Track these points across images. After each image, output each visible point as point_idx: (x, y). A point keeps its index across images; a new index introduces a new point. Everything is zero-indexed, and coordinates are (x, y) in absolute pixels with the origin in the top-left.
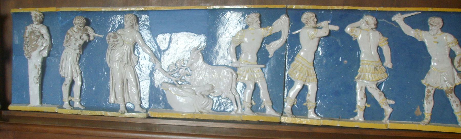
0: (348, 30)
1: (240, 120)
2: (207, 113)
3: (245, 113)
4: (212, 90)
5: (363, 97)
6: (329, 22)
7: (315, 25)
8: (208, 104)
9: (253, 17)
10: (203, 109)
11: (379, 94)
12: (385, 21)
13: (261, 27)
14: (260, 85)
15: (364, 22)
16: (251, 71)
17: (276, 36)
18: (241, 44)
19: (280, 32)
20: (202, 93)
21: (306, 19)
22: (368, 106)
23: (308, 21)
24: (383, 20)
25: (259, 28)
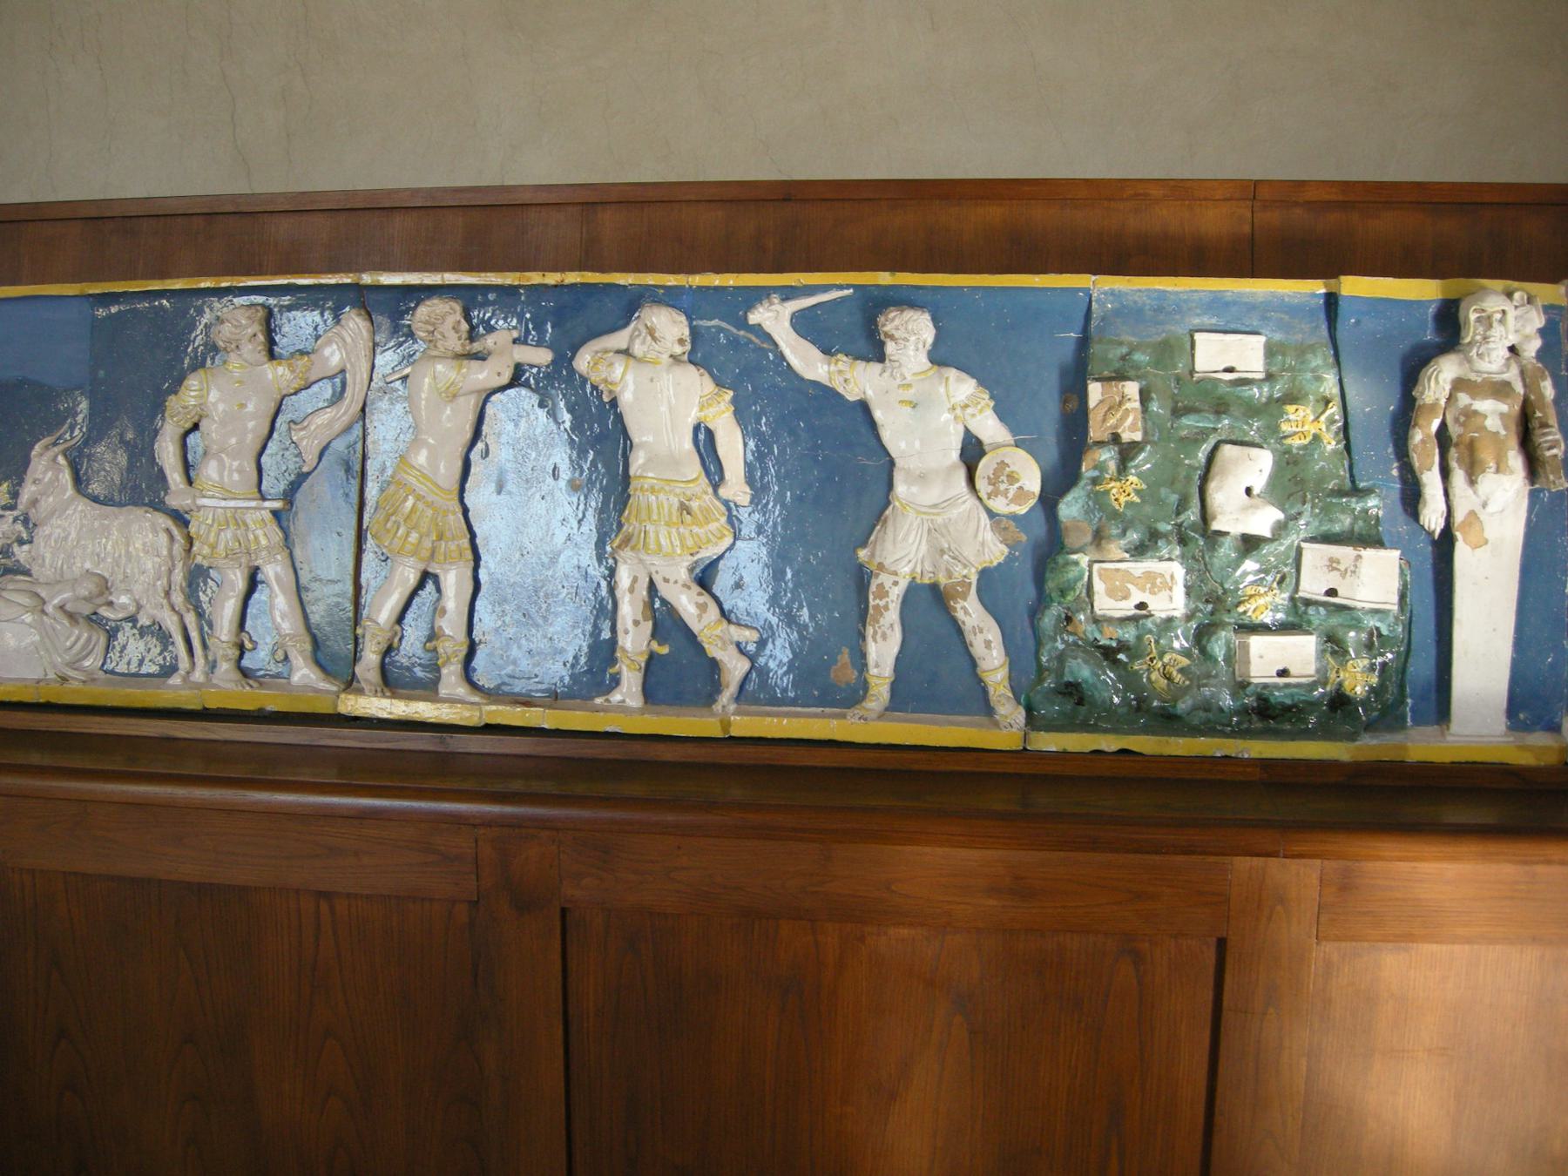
1: (198, 707)
2: (84, 682)
3: (215, 681)
4: (101, 594)
5: (640, 617)
7: (463, 345)
8: (91, 647)
9: (238, 321)
10: (71, 665)
11: (696, 603)
12: (724, 325)
15: (644, 331)
16: (238, 524)
18: (200, 421)
20: (68, 607)
21: (427, 322)
22: (664, 650)
23: (433, 332)
24: (715, 322)
25: (265, 363)
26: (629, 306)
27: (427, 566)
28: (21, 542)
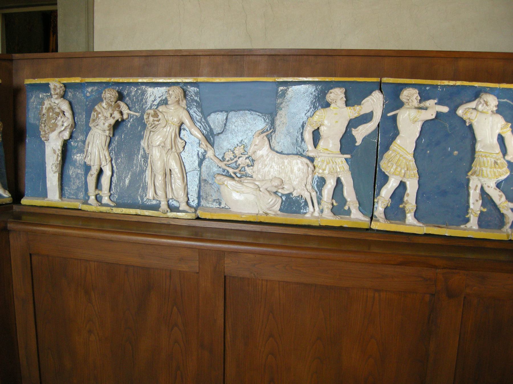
0: (460, 112)
1: (317, 224)
2: (275, 215)
3: (323, 216)
4: (281, 185)
5: (478, 199)
6: (436, 101)
7: (418, 104)
8: (276, 203)
9: (337, 93)
10: (269, 209)
11: (499, 195)
12: (508, 101)
13: (347, 105)
14: (343, 179)
15: (483, 102)
16: (333, 162)
17: (367, 118)
18: (320, 127)
19: (371, 114)
20: (268, 189)
21: (408, 96)
22: (485, 210)
23: (409, 100)
24: (505, 100)
25: (345, 108)
26: (477, 94)
27: (403, 179)
28: (248, 166)
